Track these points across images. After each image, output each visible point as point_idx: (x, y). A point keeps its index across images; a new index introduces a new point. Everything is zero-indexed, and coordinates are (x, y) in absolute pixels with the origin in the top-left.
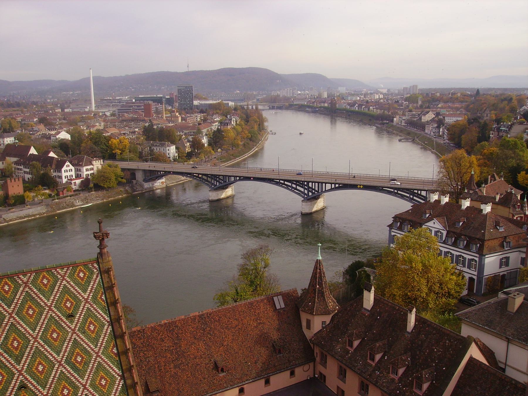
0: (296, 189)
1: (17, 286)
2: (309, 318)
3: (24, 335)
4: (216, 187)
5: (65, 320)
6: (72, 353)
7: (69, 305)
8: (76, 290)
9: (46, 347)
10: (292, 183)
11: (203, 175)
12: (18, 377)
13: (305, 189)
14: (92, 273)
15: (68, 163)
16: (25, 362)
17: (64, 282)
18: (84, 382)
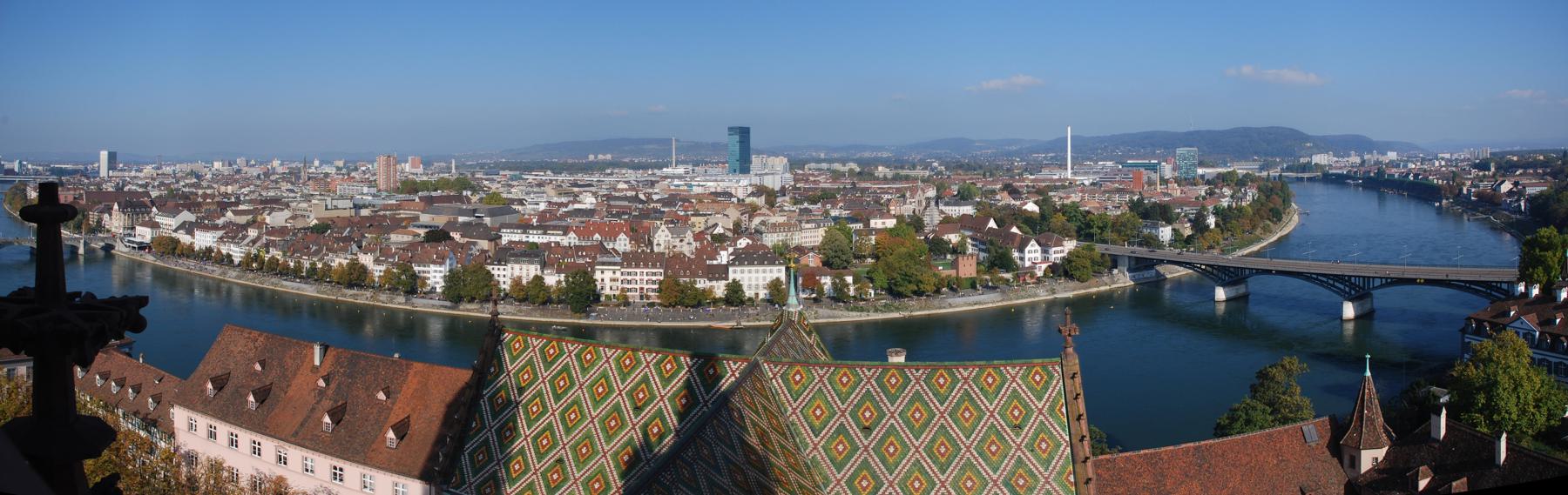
1: (955, 381)
14: (1051, 377)
15: (1033, 242)
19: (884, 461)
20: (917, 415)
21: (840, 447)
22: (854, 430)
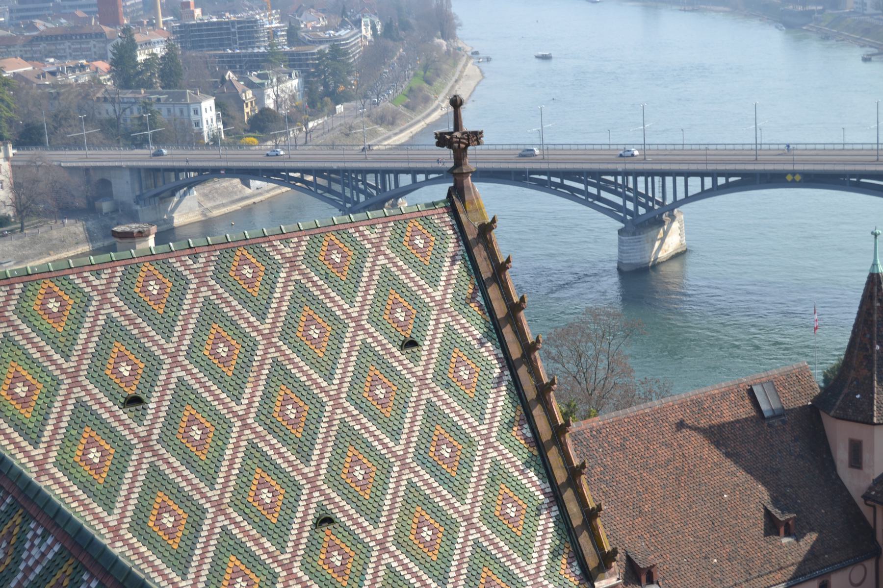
0: (598, 198)
1: (272, 269)
2: (856, 437)
3: (307, 389)
4: (359, 206)
5: (398, 354)
6: (427, 435)
7: (400, 316)
8: (412, 278)
9: (364, 420)
10: (588, 184)
11: (317, 172)
12: (310, 496)
13: (626, 198)
16: (321, 456)
17: (382, 260)
18: (465, 509)
19: (189, 462)
20: (223, 350)
21: (94, 455)
22: (109, 410)
